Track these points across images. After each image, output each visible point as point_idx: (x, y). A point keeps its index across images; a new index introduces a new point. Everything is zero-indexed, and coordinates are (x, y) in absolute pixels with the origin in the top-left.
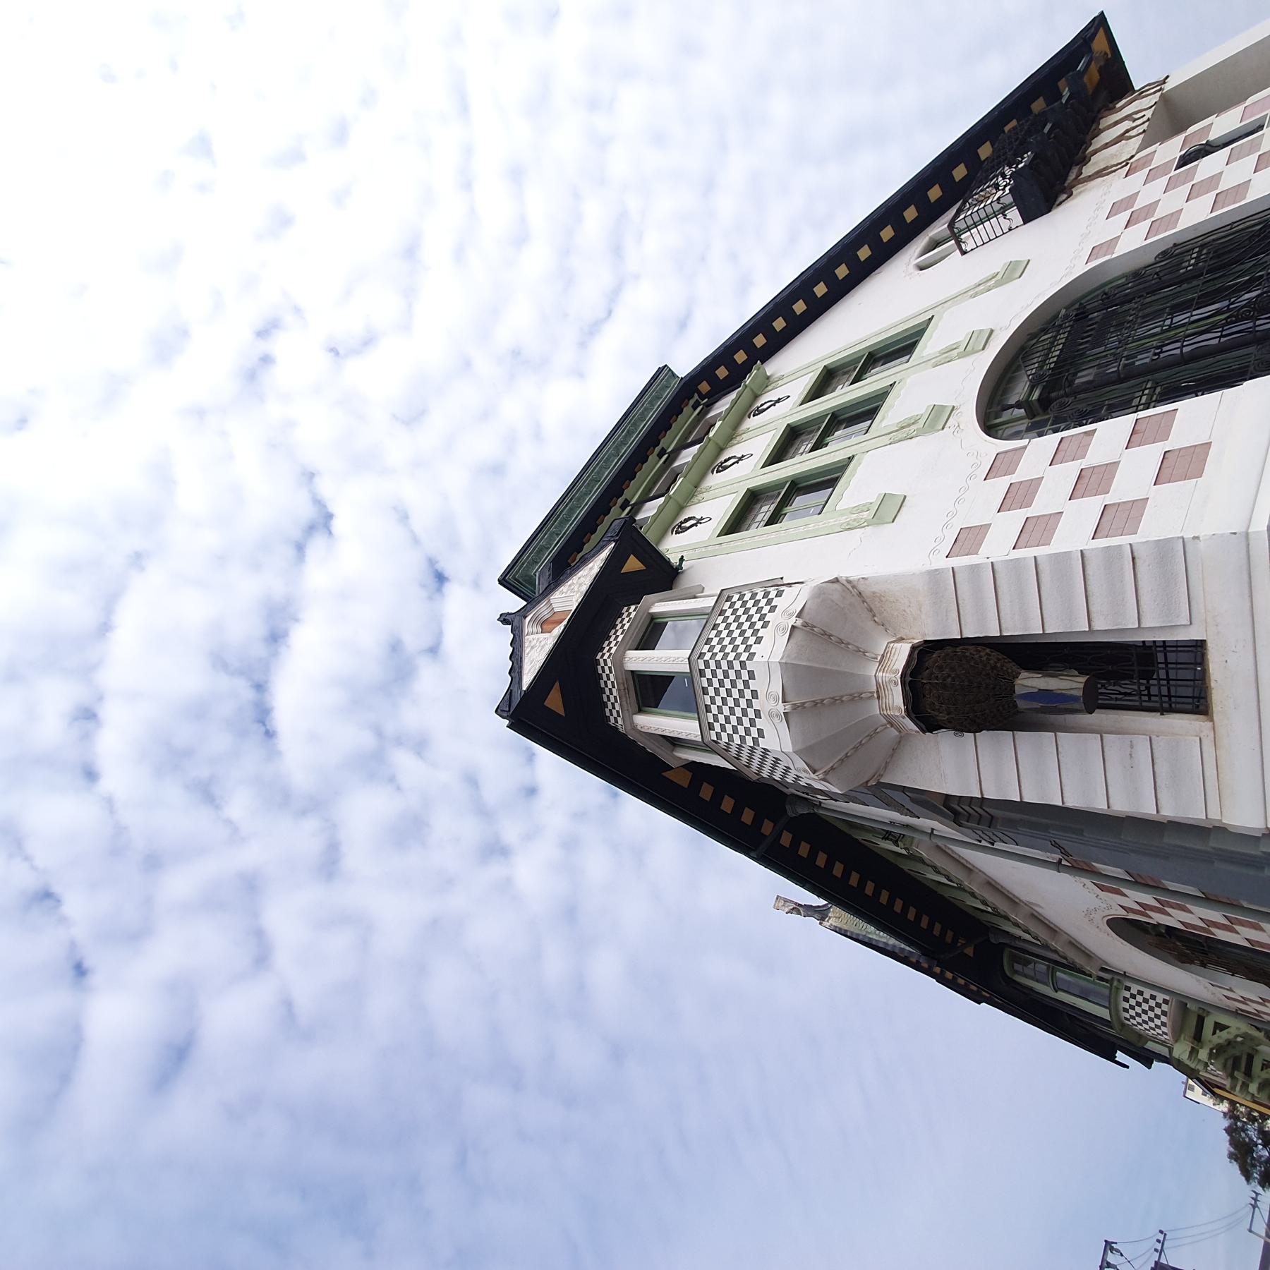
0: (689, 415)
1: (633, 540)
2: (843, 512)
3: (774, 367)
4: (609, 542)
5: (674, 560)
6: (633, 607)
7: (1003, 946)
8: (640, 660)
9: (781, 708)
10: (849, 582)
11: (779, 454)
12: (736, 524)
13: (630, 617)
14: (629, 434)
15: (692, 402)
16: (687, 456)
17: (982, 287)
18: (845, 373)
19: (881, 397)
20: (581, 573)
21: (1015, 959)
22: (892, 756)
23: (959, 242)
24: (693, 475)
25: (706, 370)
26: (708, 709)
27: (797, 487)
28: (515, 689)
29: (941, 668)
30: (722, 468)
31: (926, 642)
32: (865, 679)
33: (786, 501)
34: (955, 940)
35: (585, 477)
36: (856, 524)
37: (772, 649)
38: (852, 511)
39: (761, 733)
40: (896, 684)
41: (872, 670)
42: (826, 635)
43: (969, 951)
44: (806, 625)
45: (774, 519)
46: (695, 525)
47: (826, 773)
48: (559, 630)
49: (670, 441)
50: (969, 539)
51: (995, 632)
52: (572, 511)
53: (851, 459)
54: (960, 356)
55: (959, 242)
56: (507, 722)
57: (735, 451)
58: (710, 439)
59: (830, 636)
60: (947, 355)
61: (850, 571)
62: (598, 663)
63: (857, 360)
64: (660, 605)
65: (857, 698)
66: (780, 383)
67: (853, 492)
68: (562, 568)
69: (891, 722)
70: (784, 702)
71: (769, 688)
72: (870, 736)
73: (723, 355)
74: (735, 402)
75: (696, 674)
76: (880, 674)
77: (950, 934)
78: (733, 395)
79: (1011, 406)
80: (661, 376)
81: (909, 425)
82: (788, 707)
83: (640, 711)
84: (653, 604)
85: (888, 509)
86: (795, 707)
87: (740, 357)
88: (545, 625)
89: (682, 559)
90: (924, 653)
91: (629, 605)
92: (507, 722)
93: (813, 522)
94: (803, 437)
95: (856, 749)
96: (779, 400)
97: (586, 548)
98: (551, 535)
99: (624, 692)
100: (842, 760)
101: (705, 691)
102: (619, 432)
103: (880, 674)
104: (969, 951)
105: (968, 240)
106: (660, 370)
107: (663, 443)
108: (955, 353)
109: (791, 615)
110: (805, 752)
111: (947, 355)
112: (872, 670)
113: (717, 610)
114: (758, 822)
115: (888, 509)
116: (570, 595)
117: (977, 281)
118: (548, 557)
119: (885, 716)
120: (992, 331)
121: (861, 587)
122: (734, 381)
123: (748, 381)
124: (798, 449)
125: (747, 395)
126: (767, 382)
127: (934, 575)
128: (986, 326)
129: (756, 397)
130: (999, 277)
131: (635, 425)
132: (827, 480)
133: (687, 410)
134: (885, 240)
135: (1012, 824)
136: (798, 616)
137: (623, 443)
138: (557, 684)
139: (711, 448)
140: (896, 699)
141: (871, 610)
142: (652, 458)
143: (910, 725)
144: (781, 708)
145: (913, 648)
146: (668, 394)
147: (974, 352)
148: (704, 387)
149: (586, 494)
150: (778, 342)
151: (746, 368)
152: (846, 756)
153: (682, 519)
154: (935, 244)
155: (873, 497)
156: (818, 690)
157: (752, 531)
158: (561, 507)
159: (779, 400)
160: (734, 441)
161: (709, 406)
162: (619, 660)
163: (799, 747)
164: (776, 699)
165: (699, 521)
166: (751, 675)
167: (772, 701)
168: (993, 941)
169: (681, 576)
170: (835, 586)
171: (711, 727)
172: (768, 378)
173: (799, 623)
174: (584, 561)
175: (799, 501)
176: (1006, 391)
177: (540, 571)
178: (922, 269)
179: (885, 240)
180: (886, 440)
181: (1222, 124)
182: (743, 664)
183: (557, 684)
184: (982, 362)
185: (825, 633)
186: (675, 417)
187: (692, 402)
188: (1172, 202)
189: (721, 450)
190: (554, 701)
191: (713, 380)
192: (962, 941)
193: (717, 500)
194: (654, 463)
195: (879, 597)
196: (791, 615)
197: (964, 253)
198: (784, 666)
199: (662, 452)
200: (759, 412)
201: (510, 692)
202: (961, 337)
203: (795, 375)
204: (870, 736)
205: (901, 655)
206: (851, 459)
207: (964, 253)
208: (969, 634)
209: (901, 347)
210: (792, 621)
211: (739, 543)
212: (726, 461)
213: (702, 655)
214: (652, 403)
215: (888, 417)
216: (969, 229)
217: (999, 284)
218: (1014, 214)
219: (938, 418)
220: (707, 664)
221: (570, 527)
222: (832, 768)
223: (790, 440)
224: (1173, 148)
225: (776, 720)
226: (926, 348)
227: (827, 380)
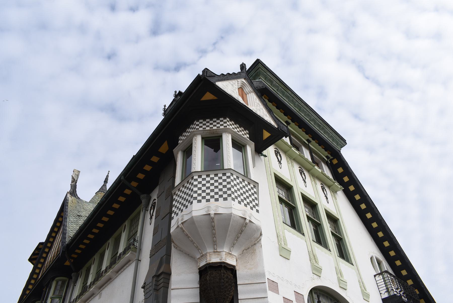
0: (324, 154)
1: (276, 136)
2: (283, 233)
3: (341, 195)
4: (278, 125)
5: (265, 152)
6: (248, 136)
7: (70, 278)
8: (227, 140)
9: (212, 212)
10: (260, 240)
11: (307, 200)
12: (280, 182)
13: (244, 135)
14: (319, 126)
15: (329, 156)
16: (307, 154)
17: (362, 284)
18: (335, 228)
19: (326, 246)
20: (268, 115)
21: (63, 282)
22: (186, 254)
23: (379, 274)
24: (299, 158)
25: (343, 163)
26: (208, 176)
27: (292, 210)
28: (216, 78)
29: (227, 277)
30: (301, 172)
31: (236, 271)
32: (222, 247)
33: (287, 204)
34: (73, 258)
35: (303, 104)
36: (280, 239)
37: (237, 209)
38: (284, 237)
39: (199, 201)
40: (221, 260)
41: (226, 250)
42: (241, 231)
43: (67, 263)
44: (246, 224)
45: (281, 200)
46: (278, 161)
47: (182, 228)
48: (240, 100)
49: (314, 145)
50: (274, 287)
51: (240, 297)
52: (287, 97)
53: (303, 234)
54: (338, 278)
55: (379, 274)
56: (201, 74)
57: (308, 179)
58: (314, 166)
59: (241, 233)
60: (339, 273)
61: (263, 239)
62: (225, 118)
63: (340, 233)
64: (249, 150)
65: (215, 244)
66: (334, 198)
67: (290, 235)
68: (264, 94)
69: (203, 256)
70: (215, 214)
71: (219, 207)
72: (197, 247)
73: (348, 171)
74: (328, 178)
75: (224, 172)
76: (224, 253)
77: (75, 256)
78: (331, 177)
79: (319, 299)
80: (342, 142)
81: (315, 259)
82: (212, 216)
83: (202, 138)
84: (251, 147)
85: (285, 253)
86: (212, 219)
87: (346, 179)
88: (241, 89)
89: (265, 156)
90: (232, 270)
91: (249, 134)
92: (201, 74)
93: (280, 219)
94: (311, 210)
95: (192, 241)
96: (327, 198)
97: (270, 104)
99: (211, 130)
100: (187, 235)
101: (216, 175)
103: (224, 253)
104: (67, 263)
106: (344, 141)
107: (313, 142)
108: (340, 276)
109: (250, 217)
110: (192, 221)
111: (339, 273)
112: (226, 250)
113: (251, 181)
114: (138, 180)
115: (285, 253)
116: (255, 105)
117: (364, 282)
118: (268, 85)
119: (206, 254)
120: (346, 290)
121: (258, 245)
122: (338, 177)
123: (337, 184)
124: (307, 208)
125: (330, 183)
126: (334, 192)
127: (263, 275)
128: (348, 288)
129: (329, 187)
130: (365, 291)
131: (323, 129)
132: (295, 224)
133: (326, 153)
134: (384, 243)
135: (157, 298)
136: (250, 221)
137: (315, 123)
138: (215, 98)
139: (310, 167)
140: (214, 259)
141: (248, 248)
142: (307, 137)
143: (202, 264)
144: (212, 212)
145: (234, 266)
146: (334, 144)
147: (339, 283)
148: (335, 161)
149: (294, 105)
150: (350, 196)
151: (341, 182)
152: (189, 237)
153: (281, 153)
154: (379, 263)
155: (290, 246)
156: (218, 228)
157: (276, 189)
159: (327, 198)
160: (312, 177)
161: (326, 163)
162: (226, 130)
163: (194, 218)
164: (216, 210)
165: (280, 162)
166: (225, 199)
167: (215, 208)
168: (73, 274)
169: (258, 155)
170: (259, 234)
171: (200, 176)
172: (336, 192)
173: (247, 221)
174: (270, 111)
175: (286, 209)
176: (323, 295)
177: (261, 81)
178: (371, 258)
179: (384, 243)
180: (310, 250)
182: (229, 195)
183: (215, 98)
184: (335, 287)
185: (242, 231)
186: (324, 148)
189: (308, 171)
190: (208, 96)
191: (338, 166)
192: (72, 261)
193: (289, 172)
194: (304, 137)
195: (254, 252)
196: (250, 217)
197: (375, 276)
198: (230, 215)
199: (308, 140)
200: (323, 189)
201: (214, 75)
202: (345, 278)
203: (336, 206)
204: (197, 247)
205: (231, 261)
206: (303, 234)
207: (375, 276)
208: (239, 288)
209: (343, 253)
210: (248, 218)
211: (272, 184)
212: (304, 174)
213: (232, 174)
214: (331, 137)
215: (318, 249)
216: (384, 278)
217: (362, 291)
218: (386, 295)
219: (317, 271)
220: (228, 177)
221: (280, 96)
222: (184, 231)
223: (311, 204)
225: (206, 209)
226: (342, 263)
227: (333, 220)
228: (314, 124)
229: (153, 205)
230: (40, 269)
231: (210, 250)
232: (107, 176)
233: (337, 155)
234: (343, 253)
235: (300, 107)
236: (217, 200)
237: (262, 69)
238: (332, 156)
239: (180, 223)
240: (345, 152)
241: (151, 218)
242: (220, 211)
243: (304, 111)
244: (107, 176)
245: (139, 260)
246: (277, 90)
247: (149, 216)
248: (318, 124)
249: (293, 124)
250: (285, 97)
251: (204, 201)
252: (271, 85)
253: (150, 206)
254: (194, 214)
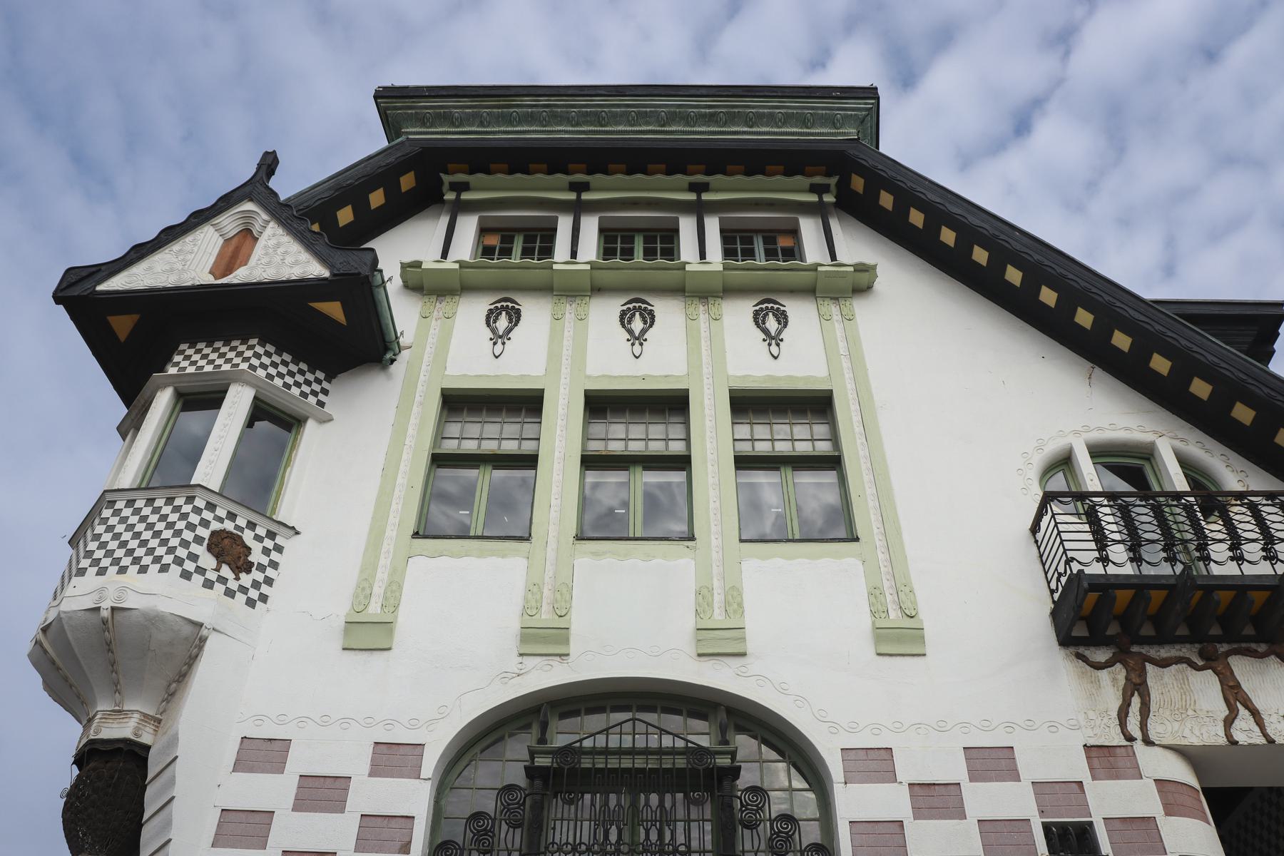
14: (711, 119)
15: (818, 180)
52: (530, 119)
98: (475, 116)
131: (732, 118)
137: (686, 119)
149: (569, 121)
187: (818, 180)
199: (693, 187)
221: (501, 133)
228: (688, 124)
235: (596, 114)
237: (396, 108)
238: (828, 175)
243: (615, 115)
246: (482, 124)
248: (704, 115)
250: (519, 123)
252: (453, 125)
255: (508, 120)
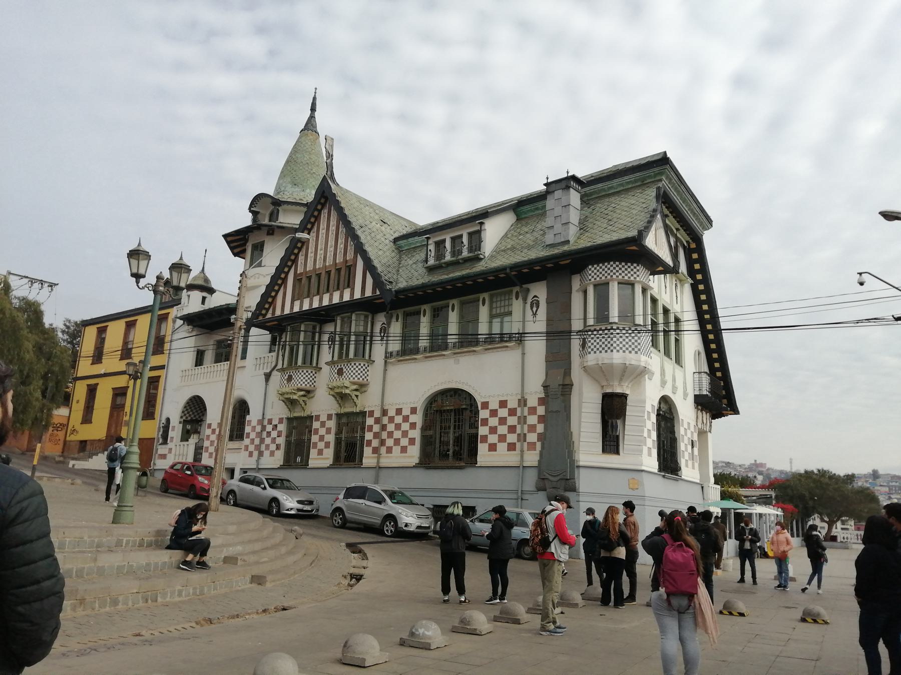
14: (694, 214)
21: (366, 317)
39: (618, 351)
52: (678, 192)
65: (621, 380)
102: (698, 209)
105: (696, 375)
106: (710, 221)
110: (611, 366)
127: (644, 402)
129: (681, 281)
140: (618, 390)
143: (609, 390)
148: (693, 246)
158: (682, 187)
181: (696, 450)
188: (686, 438)
199: (677, 230)
223: (666, 311)
224: (695, 438)
229: (536, 304)
230: (287, 273)
231: (616, 383)
232: (314, 99)
233: (697, 239)
234: (678, 361)
236: (630, 352)
239: (600, 363)
240: (709, 238)
241: (535, 314)
242: (633, 362)
244: (314, 99)
245: (523, 354)
247: (529, 313)
249: (671, 217)
251: (621, 351)
253: (529, 301)
254: (615, 361)
255: (676, 189)
